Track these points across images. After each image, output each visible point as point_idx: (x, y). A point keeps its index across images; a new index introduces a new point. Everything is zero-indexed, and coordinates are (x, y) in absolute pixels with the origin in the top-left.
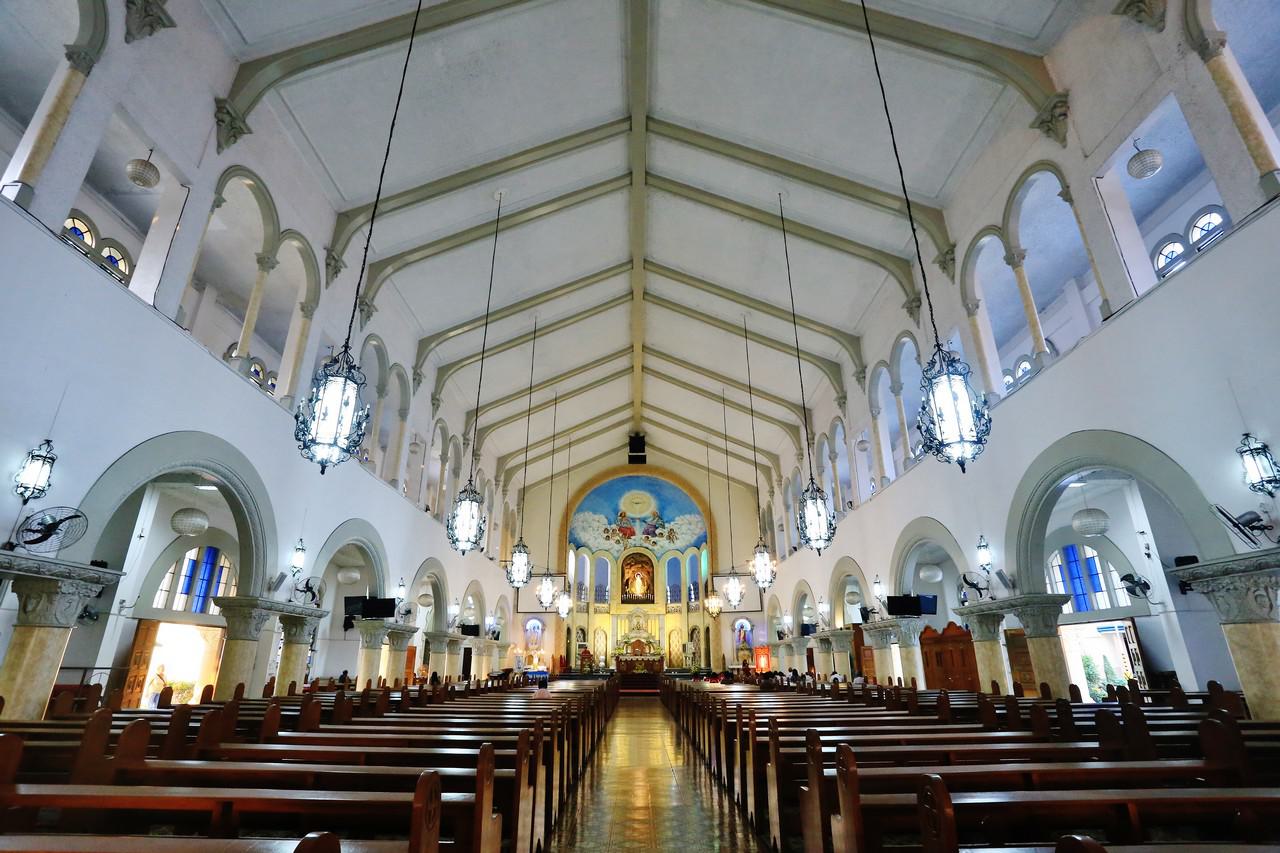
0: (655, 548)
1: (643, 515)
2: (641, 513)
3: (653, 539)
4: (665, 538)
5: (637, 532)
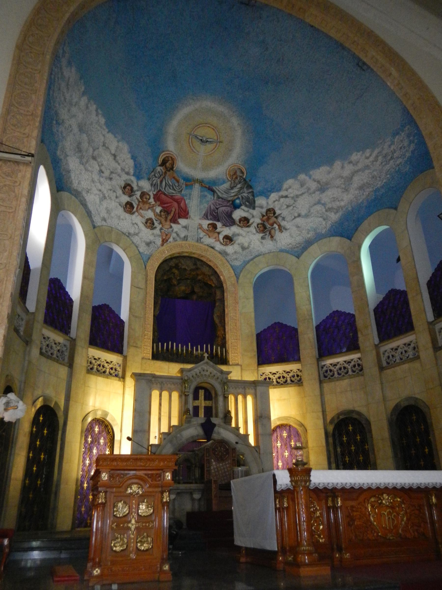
0: (230, 249)
1: (212, 174)
2: (206, 167)
3: (227, 231)
4: (252, 229)
5: (191, 214)
